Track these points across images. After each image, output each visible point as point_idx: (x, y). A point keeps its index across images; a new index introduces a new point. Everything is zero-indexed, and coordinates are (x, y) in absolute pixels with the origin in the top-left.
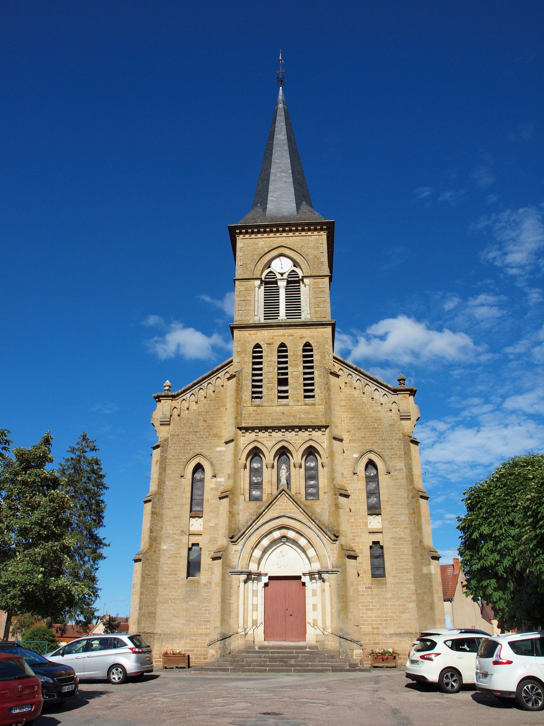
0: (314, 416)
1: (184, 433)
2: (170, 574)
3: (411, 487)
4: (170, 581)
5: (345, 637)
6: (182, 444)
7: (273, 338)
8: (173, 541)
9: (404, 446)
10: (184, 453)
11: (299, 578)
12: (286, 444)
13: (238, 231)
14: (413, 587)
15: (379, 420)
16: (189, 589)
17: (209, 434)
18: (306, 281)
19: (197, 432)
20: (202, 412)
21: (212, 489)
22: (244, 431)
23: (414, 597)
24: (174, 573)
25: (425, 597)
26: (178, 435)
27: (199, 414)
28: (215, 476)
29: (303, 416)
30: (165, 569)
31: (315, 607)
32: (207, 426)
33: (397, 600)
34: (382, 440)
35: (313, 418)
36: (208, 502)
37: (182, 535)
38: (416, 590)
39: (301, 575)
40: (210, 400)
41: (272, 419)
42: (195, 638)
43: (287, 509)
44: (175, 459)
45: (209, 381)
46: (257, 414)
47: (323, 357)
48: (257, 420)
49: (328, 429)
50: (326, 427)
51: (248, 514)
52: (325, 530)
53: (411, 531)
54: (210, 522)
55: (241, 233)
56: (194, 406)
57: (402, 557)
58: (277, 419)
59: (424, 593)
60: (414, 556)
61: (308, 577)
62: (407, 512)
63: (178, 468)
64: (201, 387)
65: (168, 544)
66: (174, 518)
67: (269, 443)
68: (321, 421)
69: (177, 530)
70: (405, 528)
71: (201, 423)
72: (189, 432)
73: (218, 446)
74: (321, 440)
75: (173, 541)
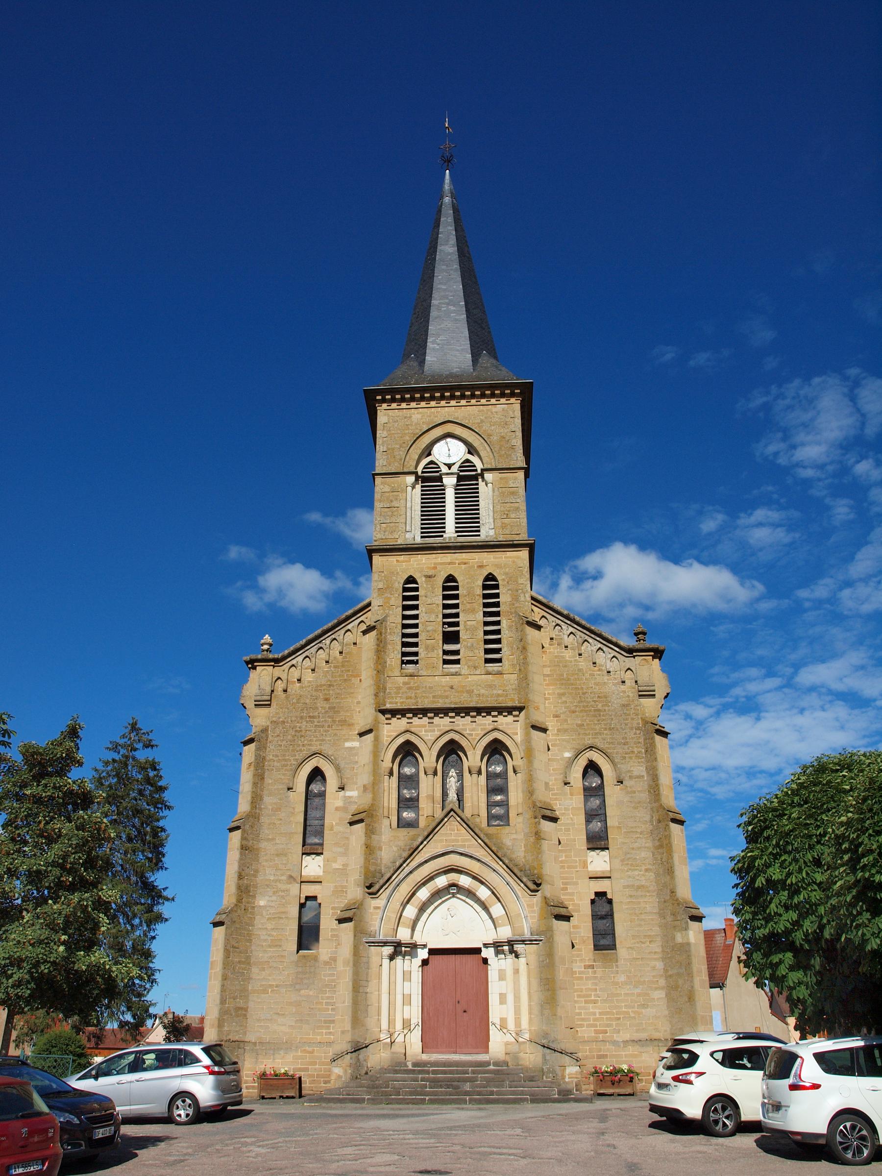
0: (500, 692)
1: (293, 719)
2: (270, 946)
3: (656, 805)
4: (271, 957)
5: (552, 1045)
6: (289, 737)
7: (435, 568)
8: (274, 893)
9: (645, 740)
10: (293, 751)
11: (477, 951)
12: (456, 737)
13: (379, 397)
14: (660, 965)
15: (604, 698)
16: (300, 969)
17: (334, 721)
18: (488, 476)
19: (313, 717)
20: (321, 686)
21: (337, 809)
22: (389, 716)
23: (662, 982)
24: (276, 944)
25: (680, 982)
26: (283, 722)
27: (318, 688)
28: (343, 789)
29: (483, 691)
30: (262, 937)
31: (503, 999)
32: (329, 708)
33: (635, 987)
34: (610, 729)
35: (498, 696)
36: (332, 829)
37: (290, 883)
38: (666, 971)
39: (481, 946)
40: (335, 667)
41: (434, 697)
42: (310, 1049)
43: (457, 841)
44: (279, 761)
45: (333, 636)
46: (410, 688)
47: (516, 598)
48: (411, 698)
49: (523, 713)
50: (520, 709)
51: (395, 849)
52: (519, 874)
53: (657, 875)
54: (335, 862)
55: (384, 401)
56: (308, 677)
57: (643, 917)
58: (441, 697)
59: (678, 974)
60: (662, 916)
61: (491, 950)
62: (650, 844)
63: (284, 774)
64: (320, 645)
65: (267, 898)
66: (277, 855)
67: (429, 734)
68: (513, 700)
69: (282, 875)
70: (646, 870)
71: (320, 704)
72: (302, 718)
73: (347, 740)
74: (512, 729)
75: (274, 893)
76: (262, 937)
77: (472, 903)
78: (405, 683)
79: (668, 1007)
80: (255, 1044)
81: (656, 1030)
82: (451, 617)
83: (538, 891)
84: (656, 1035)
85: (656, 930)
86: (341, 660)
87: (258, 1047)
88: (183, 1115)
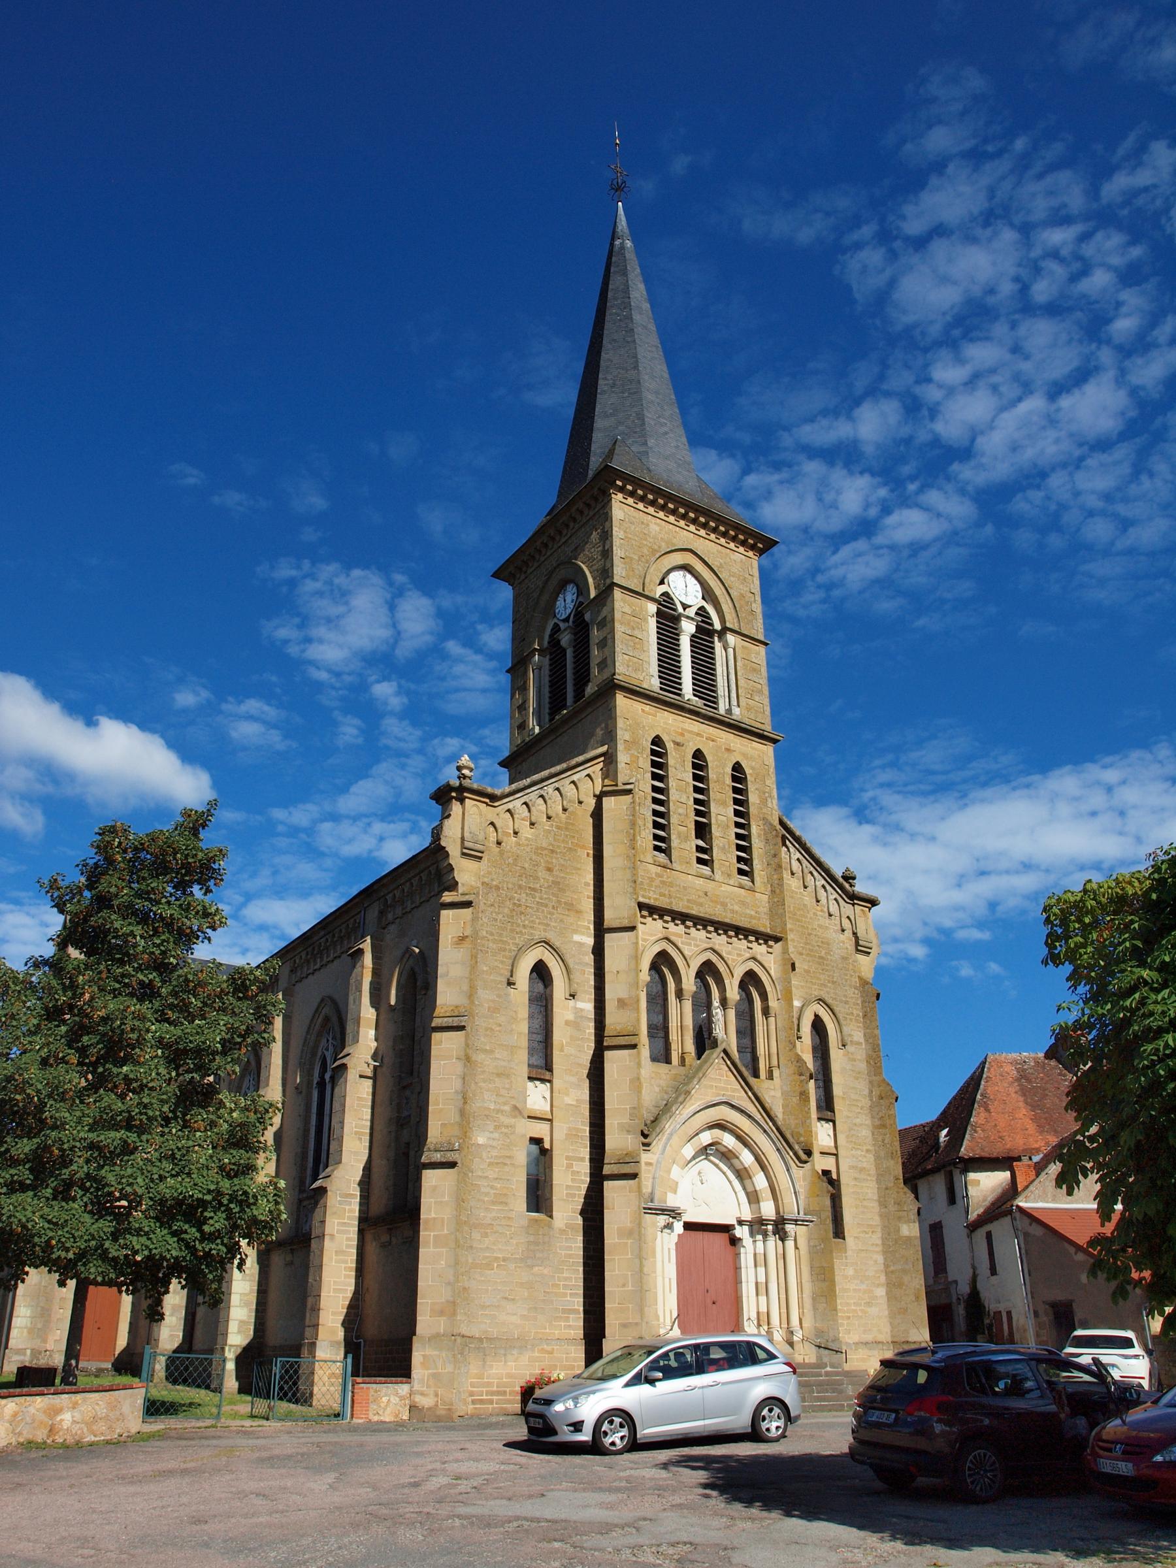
0: (753, 913)
1: (510, 886)
2: (493, 1203)
3: (877, 1078)
4: (495, 1219)
5: (831, 1345)
6: (506, 910)
7: (682, 735)
8: (497, 1128)
9: (863, 1002)
10: (512, 931)
11: (726, 1229)
12: (714, 959)
13: (619, 483)
14: (880, 1258)
15: (826, 943)
16: (532, 1238)
17: (559, 902)
18: (731, 638)
19: (534, 890)
20: (543, 849)
21: (567, 1023)
22: (645, 913)
23: (883, 1279)
24: (501, 1199)
25: (906, 1279)
26: (498, 888)
27: (538, 850)
28: (573, 996)
29: (736, 908)
30: (483, 1190)
31: (762, 1289)
32: (553, 882)
33: (862, 1282)
34: (834, 983)
35: (751, 917)
36: (562, 1050)
37: (515, 1117)
38: (886, 1266)
39: (735, 1223)
40: (558, 828)
41: (688, 901)
42: (549, 1348)
43: (727, 1090)
44: (494, 941)
45: (556, 785)
46: (663, 882)
47: (764, 802)
48: (664, 895)
49: (780, 944)
50: (777, 939)
51: (657, 1089)
52: (791, 1140)
53: (877, 1158)
54: (567, 1095)
55: (622, 490)
56: (526, 832)
57: (865, 1203)
58: (695, 902)
59: (904, 1271)
60: (883, 1203)
61: (746, 1228)
62: (868, 1122)
63: (502, 962)
64: (542, 792)
65: (487, 1134)
66: (498, 1075)
67: (693, 947)
68: (765, 926)
69: (505, 1104)
70: (867, 1151)
71: (542, 873)
72: (520, 887)
73: (576, 932)
74: (769, 959)
75: (497, 1128)
76: (483, 1190)
77: (725, 1168)
78: (658, 875)
79: (889, 1306)
80: (480, 1340)
81: (880, 1331)
82: (702, 807)
83: (806, 1162)
84: (881, 1338)
85: (877, 1220)
86: (564, 820)
87: (485, 1345)
88: (618, 1441)
